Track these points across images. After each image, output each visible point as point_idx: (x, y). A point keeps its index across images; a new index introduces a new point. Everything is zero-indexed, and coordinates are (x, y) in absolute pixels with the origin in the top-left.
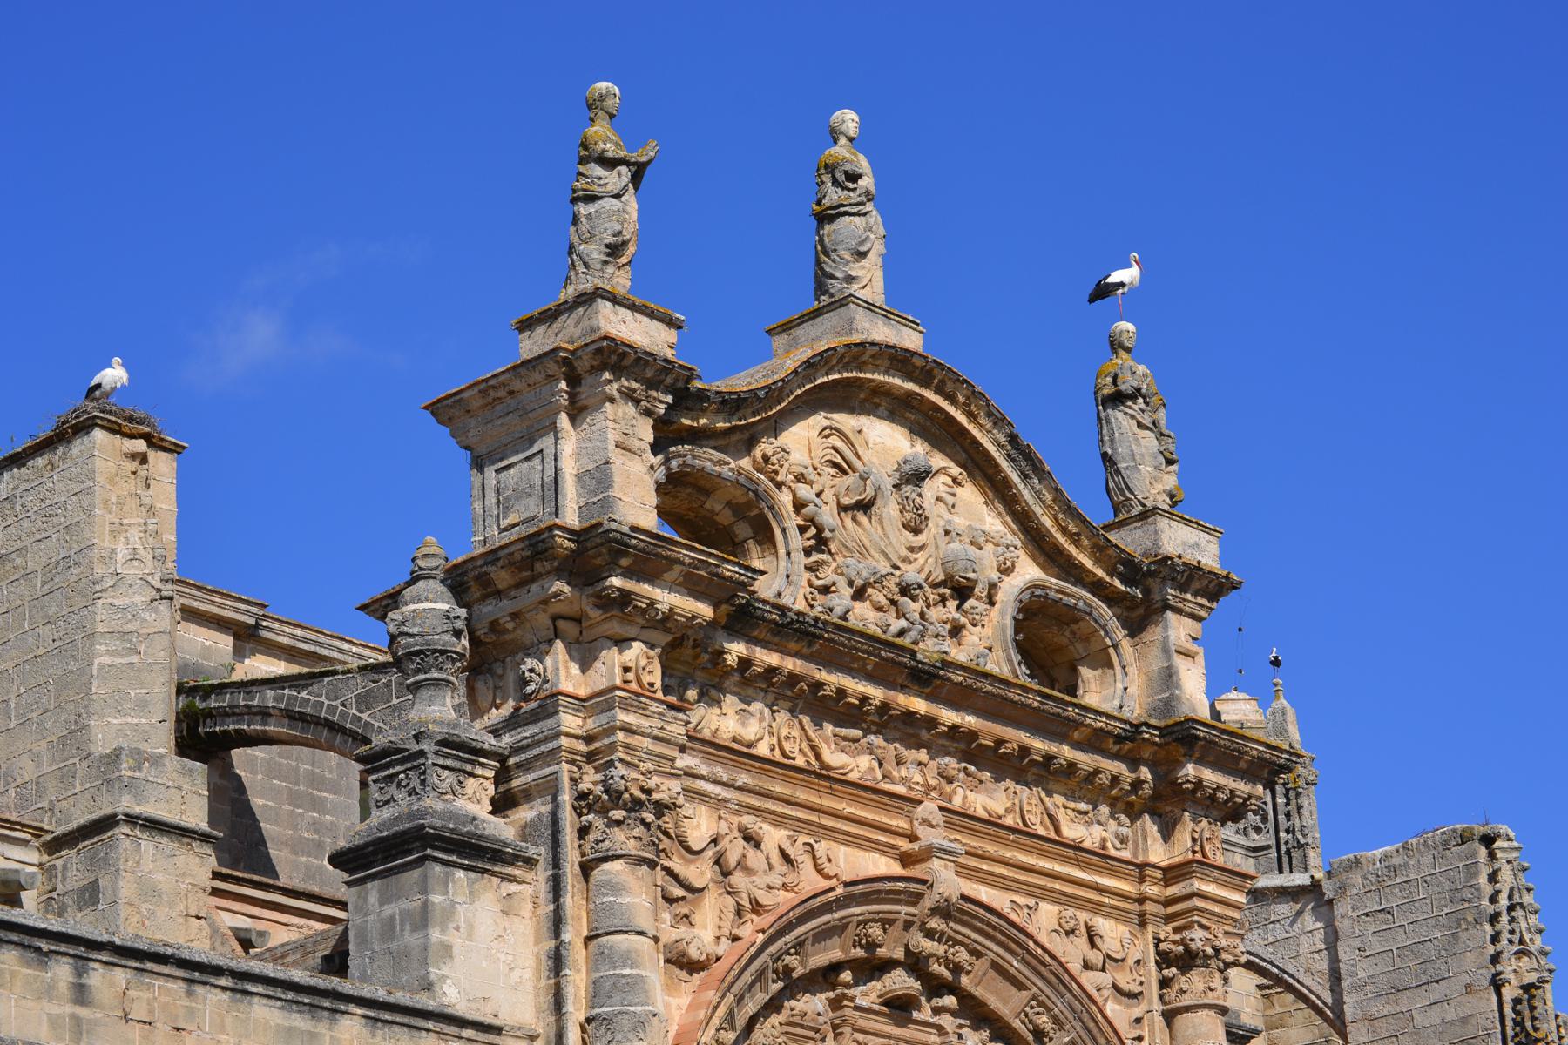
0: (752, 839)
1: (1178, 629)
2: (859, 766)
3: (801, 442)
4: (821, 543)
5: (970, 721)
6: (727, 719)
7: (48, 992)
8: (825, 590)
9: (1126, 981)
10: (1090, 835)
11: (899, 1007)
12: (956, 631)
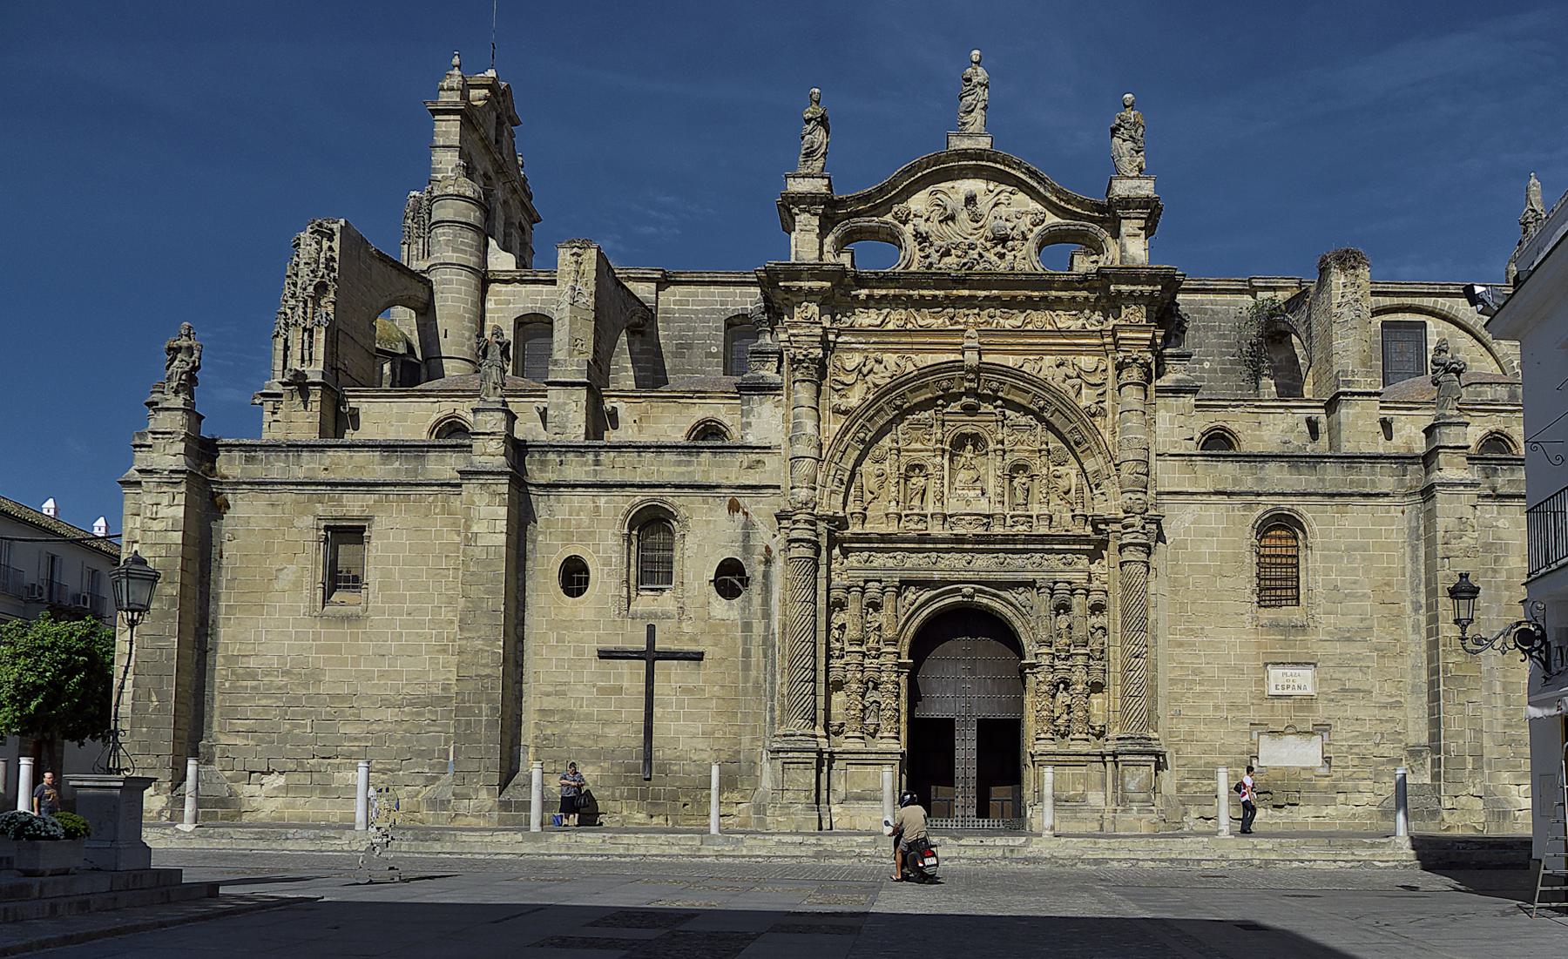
0: (879, 362)
1: (1127, 227)
2: (936, 323)
3: (919, 202)
4: (926, 239)
5: (995, 292)
6: (867, 319)
7: (585, 464)
8: (927, 257)
9: (1092, 380)
10: (1075, 325)
11: (970, 410)
12: (1002, 256)
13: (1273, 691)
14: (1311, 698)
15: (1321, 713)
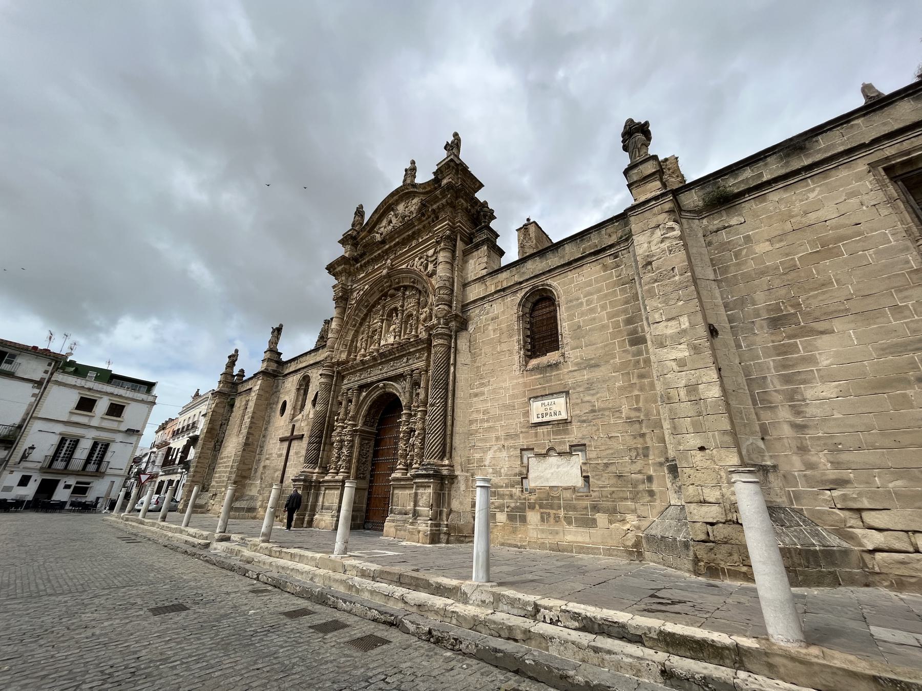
13: (536, 420)
14: (565, 422)
15: (576, 434)
